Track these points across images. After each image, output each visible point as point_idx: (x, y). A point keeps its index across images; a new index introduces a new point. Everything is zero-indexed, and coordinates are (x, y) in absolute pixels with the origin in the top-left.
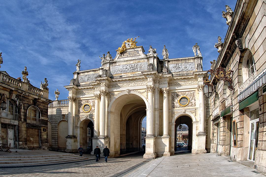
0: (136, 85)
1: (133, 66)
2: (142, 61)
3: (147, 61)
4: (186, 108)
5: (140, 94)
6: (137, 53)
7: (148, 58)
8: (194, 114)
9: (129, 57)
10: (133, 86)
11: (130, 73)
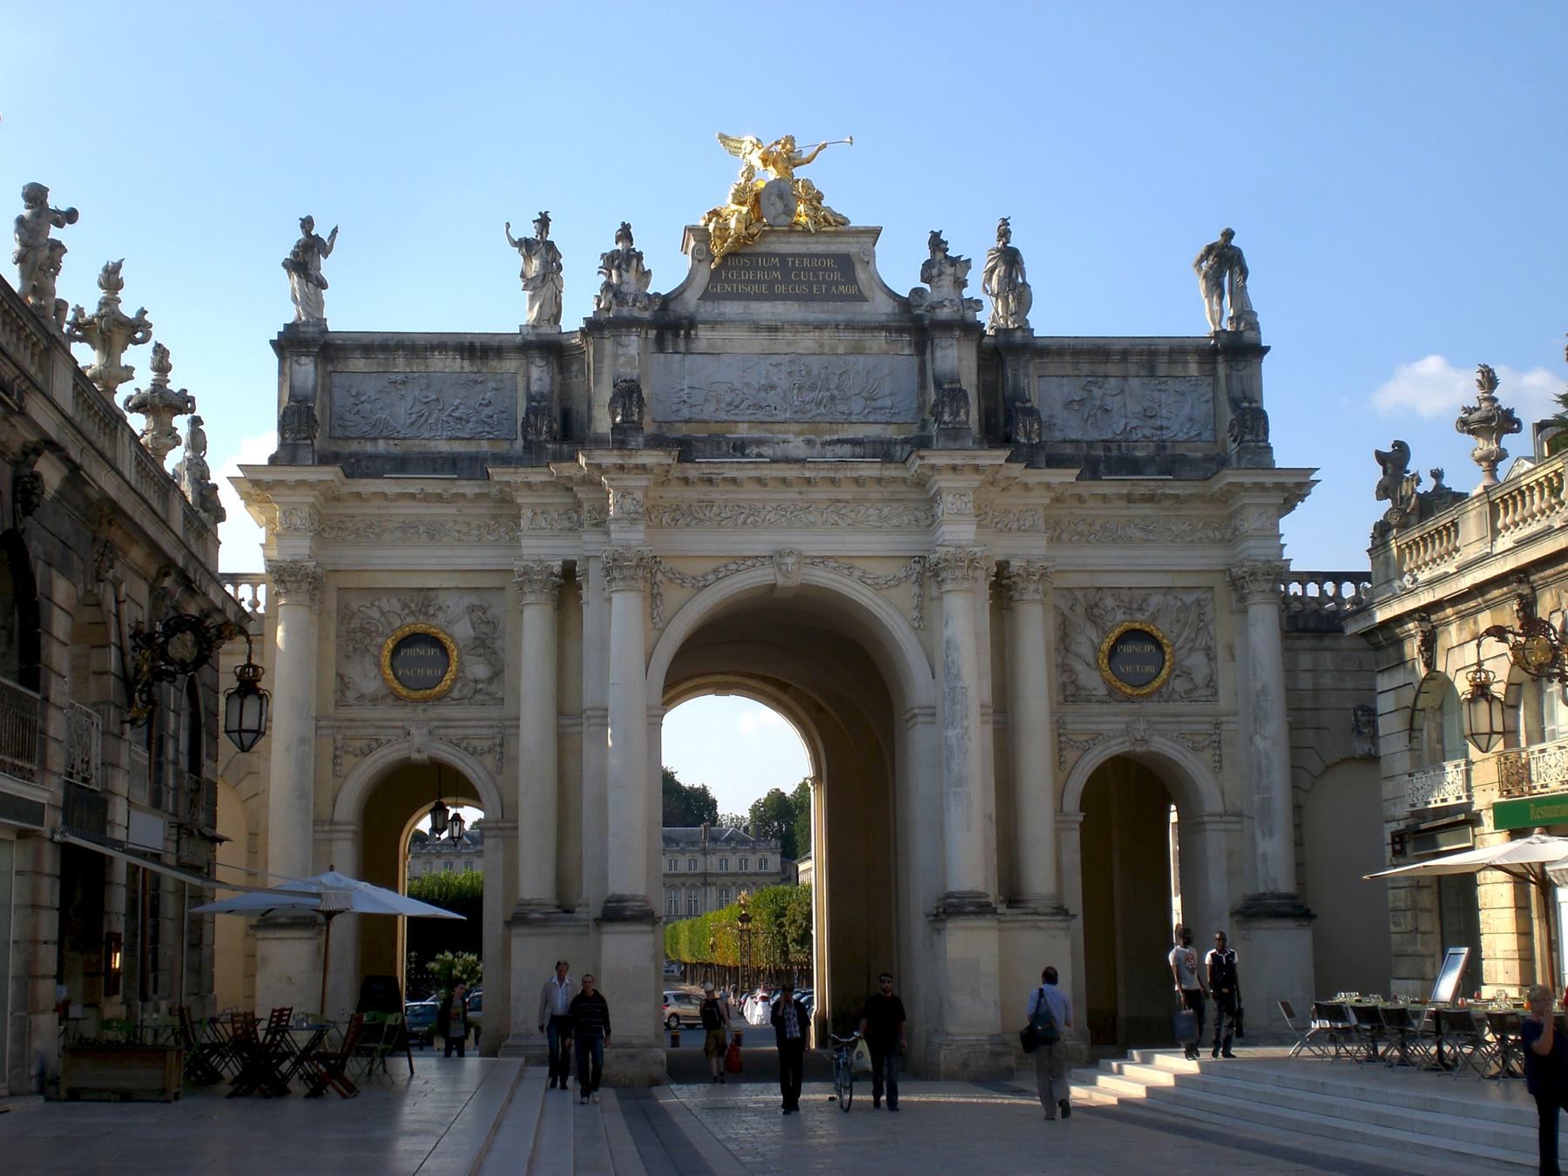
1: (815, 372)
2: (878, 342)
4: (1151, 707)
5: (869, 594)
6: (837, 276)
8: (1208, 755)
11: (797, 427)
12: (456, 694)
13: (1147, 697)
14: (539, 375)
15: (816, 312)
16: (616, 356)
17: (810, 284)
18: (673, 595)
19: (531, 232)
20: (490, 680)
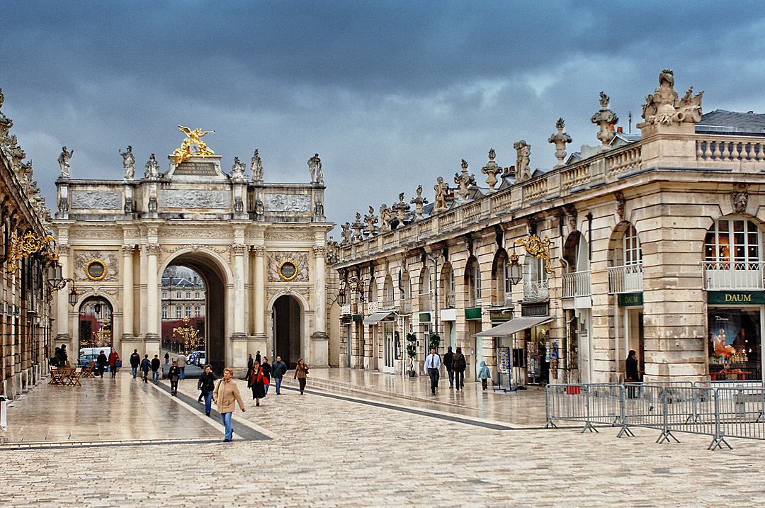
0: (210, 236)
2: (220, 187)
3: (229, 189)
6: (210, 169)
7: (232, 185)
9: (195, 174)
10: (203, 237)
12: (105, 279)
13: (290, 280)
14: (128, 193)
15: (204, 179)
16: (150, 190)
17: (202, 171)
18: (165, 255)
19: (126, 152)
20: (115, 275)
